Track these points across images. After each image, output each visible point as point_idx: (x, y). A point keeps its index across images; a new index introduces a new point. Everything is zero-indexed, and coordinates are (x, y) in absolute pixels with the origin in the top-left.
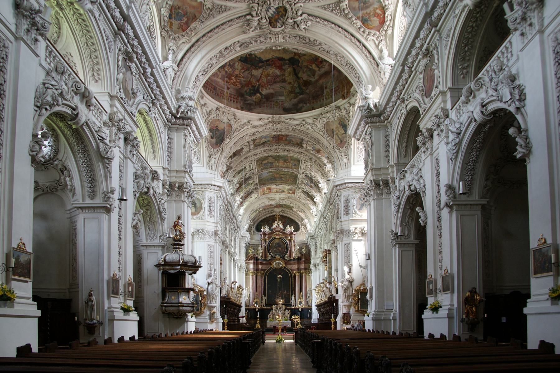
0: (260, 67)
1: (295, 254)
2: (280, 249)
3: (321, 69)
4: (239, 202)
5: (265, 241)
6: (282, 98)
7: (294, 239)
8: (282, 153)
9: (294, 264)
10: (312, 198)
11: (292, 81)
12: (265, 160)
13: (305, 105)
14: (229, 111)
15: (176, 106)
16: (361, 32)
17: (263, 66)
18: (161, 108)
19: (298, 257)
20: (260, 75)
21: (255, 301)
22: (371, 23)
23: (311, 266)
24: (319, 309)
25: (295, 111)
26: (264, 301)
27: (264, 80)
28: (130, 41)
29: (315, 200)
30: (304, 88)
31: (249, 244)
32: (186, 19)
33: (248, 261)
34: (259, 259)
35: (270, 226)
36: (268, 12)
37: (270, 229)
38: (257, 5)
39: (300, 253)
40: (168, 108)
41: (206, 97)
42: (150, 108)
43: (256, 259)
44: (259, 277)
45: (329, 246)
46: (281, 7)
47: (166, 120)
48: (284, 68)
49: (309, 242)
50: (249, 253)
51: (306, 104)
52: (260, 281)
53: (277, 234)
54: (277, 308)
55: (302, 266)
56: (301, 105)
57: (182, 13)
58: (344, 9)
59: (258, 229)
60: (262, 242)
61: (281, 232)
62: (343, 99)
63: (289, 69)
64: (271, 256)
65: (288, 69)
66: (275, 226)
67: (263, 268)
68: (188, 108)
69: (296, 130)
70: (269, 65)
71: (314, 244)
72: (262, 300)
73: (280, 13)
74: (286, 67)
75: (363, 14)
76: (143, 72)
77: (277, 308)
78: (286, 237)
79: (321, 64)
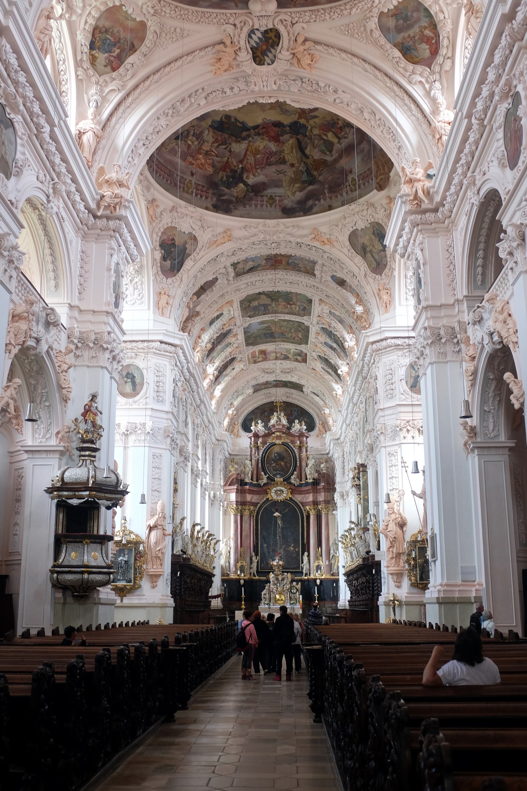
0: (244, 139)
1: (310, 473)
2: (283, 463)
4: (211, 377)
5: (258, 448)
7: (305, 445)
8: (282, 288)
9: (307, 492)
10: (335, 369)
12: (254, 300)
13: (317, 202)
14: (192, 212)
15: (95, 197)
16: (401, 70)
17: (249, 136)
18: (69, 198)
19: (314, 479)
20: (244, 152)
21: (239, 564)
22: (416, 54)
23: (337, 496)
24: (350, 581)
25: (302, 213)
26: (255, 565)
27: (251, 159)
28: (13, 74)
29: (339, 372)
31: (229, 454)
32: (118, 51)
33: (227, 488)
34: (246, 484)
35: (266, 421)
36: (250, 39)
37: (266, 426)
38: (233, 27)
39: (317, 471)
40: (81, 199)
41: (155, 189)
42: (48, 197)
43: (242, 483)
44: (246, 518)
45: (364, 456)
46: (271, 29)
47: (78, 221)
49: (331, 452)
50: (230, 471)
51: (319, 200)
52: (248, 526)
53: (277, 436)
54: (277, 579)
55: (321, 497)
56: (310, 202)
57: (112, 39)
58: (371, 31)
59: (246, 427)
60: (251, 451)
61: (284, 433)
62: (378, 191)
64: (268, 478)
66: (273, 422)
67: (253, 501)
68: (117, 200)
69: (303, 246)
70: (258, 134)
71: (341, 454)
72: (251, 563)
73: (271, 41)
75: (404, 38)
76: (36, 132)
77: (277, 579)
78: (293, 442)
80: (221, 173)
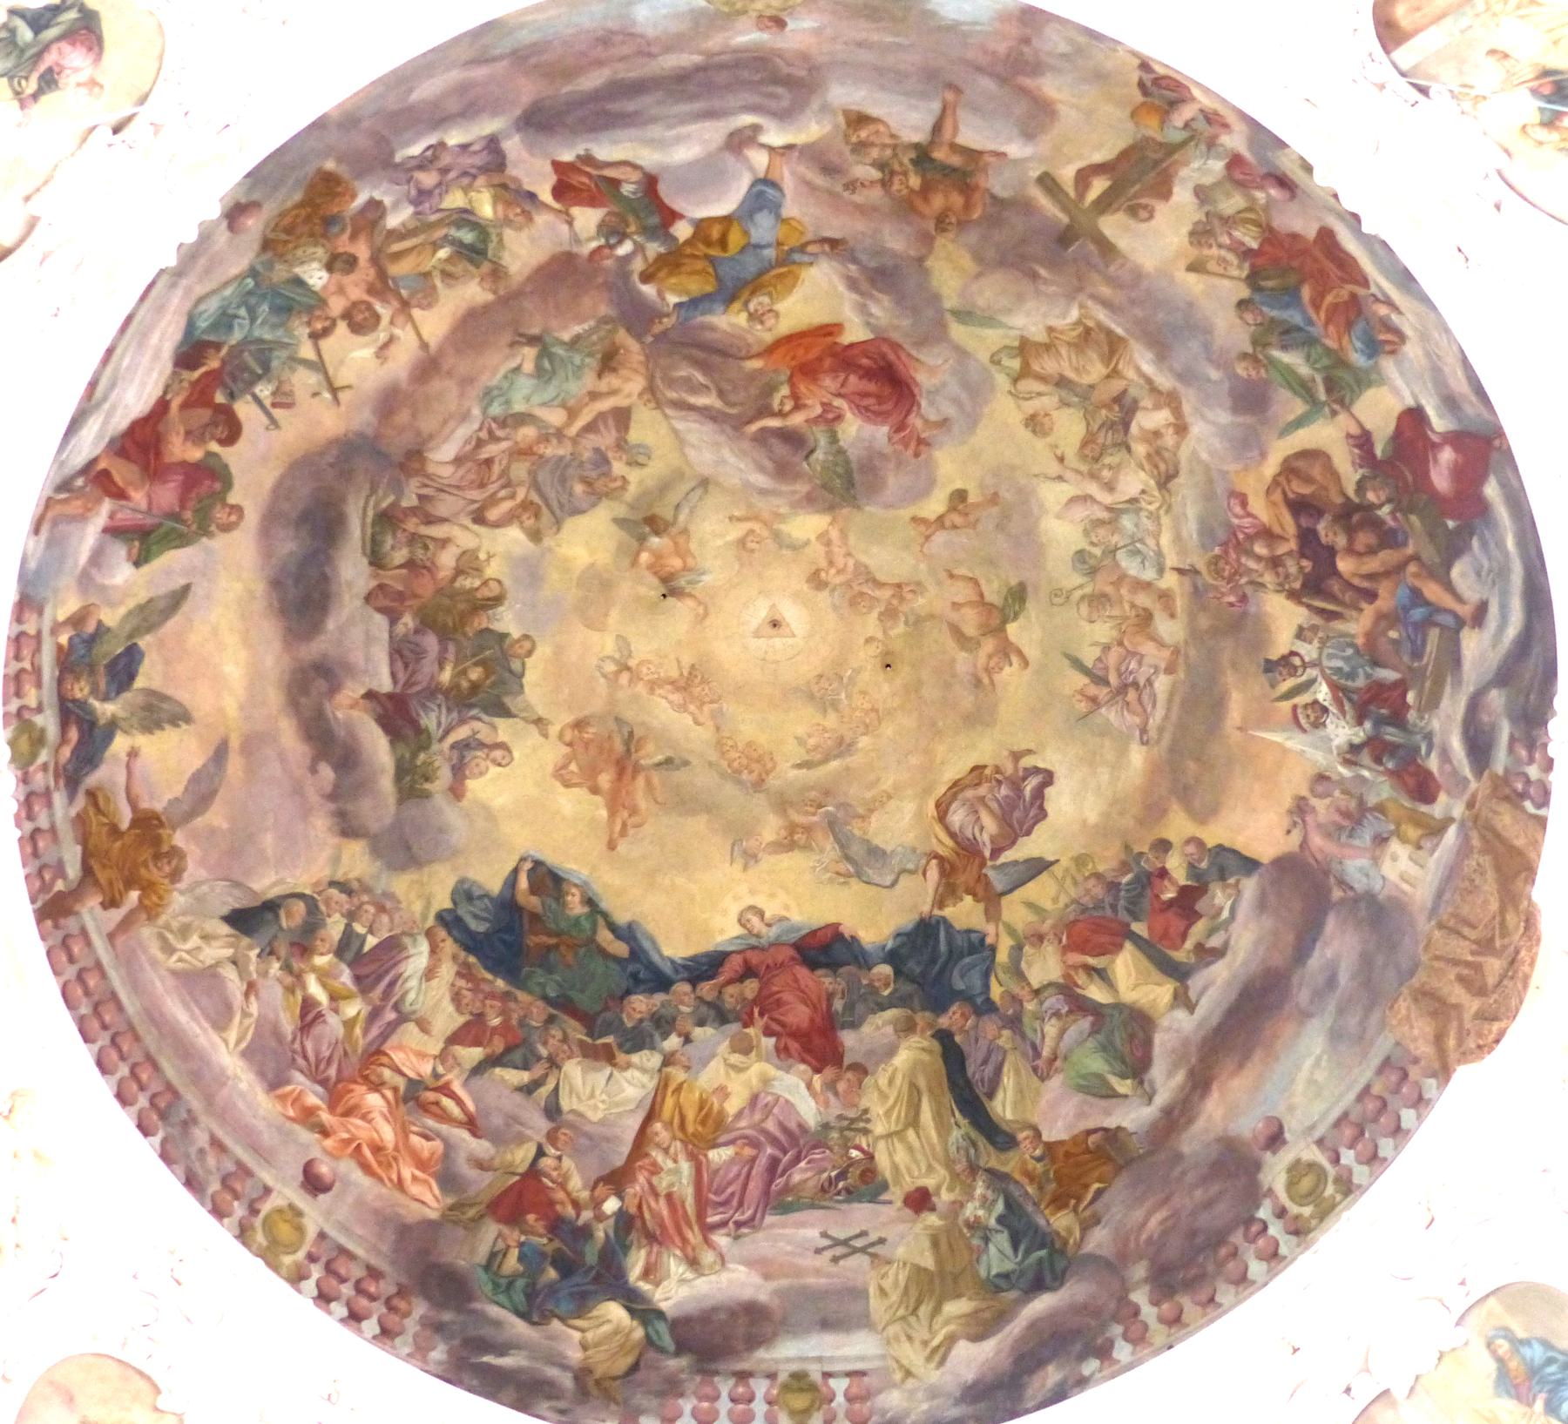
0: (637, 1040)
3: (1195, 983)
6: (857, 1348)
11: (935, 1180)
17: (664, 1023)
30: (1062, 1221)
48: (848, 1038)
63: (903, 1058)
65: (891, 1051)
74: (878, 1027)
79: (1192, 916)
80: (491, 1231)
